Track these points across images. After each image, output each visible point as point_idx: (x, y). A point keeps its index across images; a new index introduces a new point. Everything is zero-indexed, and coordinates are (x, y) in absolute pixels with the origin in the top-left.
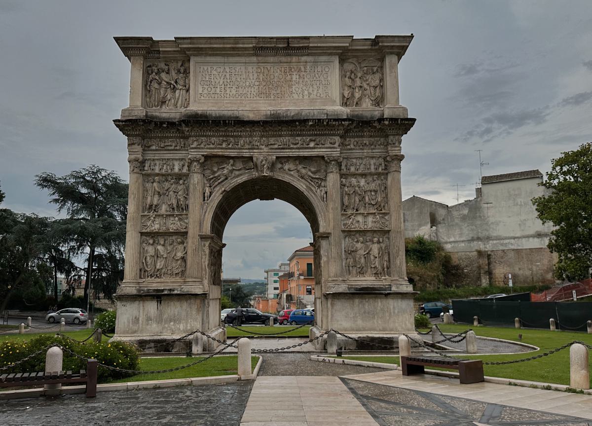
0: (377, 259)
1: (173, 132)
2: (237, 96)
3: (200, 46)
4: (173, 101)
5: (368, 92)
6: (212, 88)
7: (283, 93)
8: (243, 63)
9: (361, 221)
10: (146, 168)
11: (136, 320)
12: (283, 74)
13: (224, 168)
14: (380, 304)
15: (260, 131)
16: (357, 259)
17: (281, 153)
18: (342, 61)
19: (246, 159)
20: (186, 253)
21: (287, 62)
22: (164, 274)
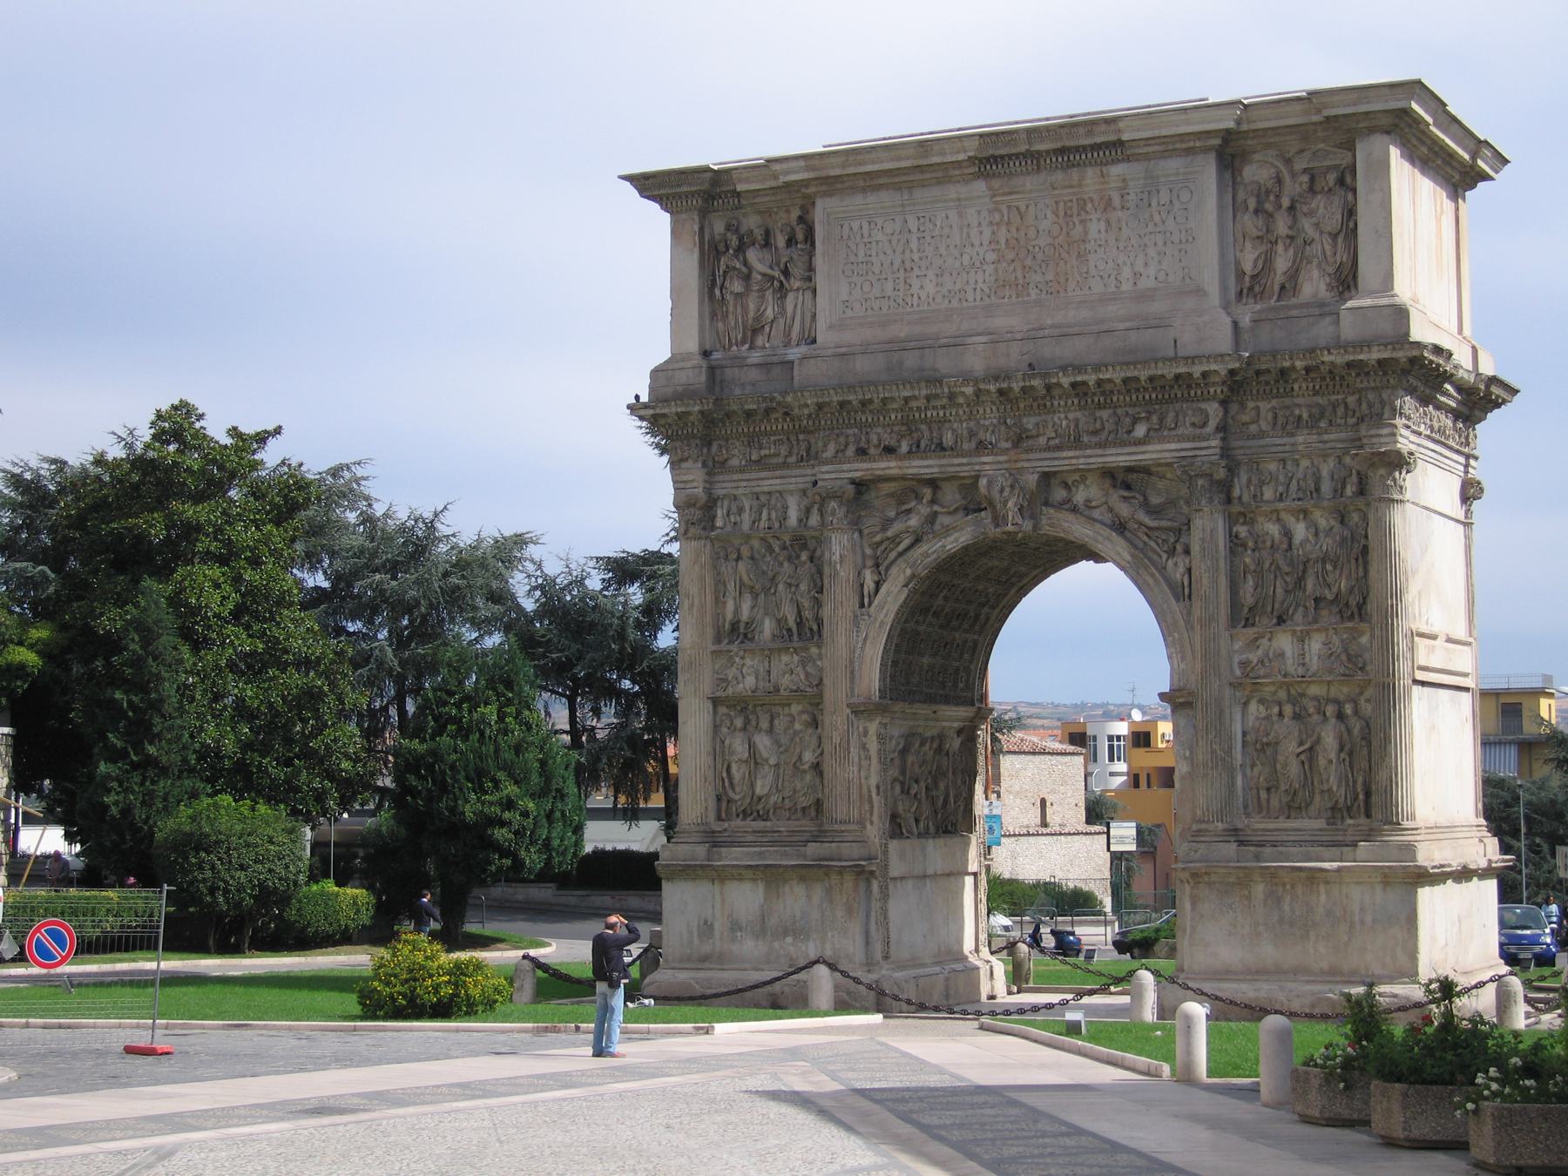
0: (1333, 767)
2: (939, 299)
3: (833, 173)
4: (782, 321)
5: (1316, 248)
7: (1062, 281)
8: (953, 200)
9: (1289, 652)
10: (719, 523)
11: (707, 928)
14: (1323, 898)
16: (1278, 766)
17: (1056, 463)
20: (822, 754)
21: (1071, 187)
22: (775, 809)
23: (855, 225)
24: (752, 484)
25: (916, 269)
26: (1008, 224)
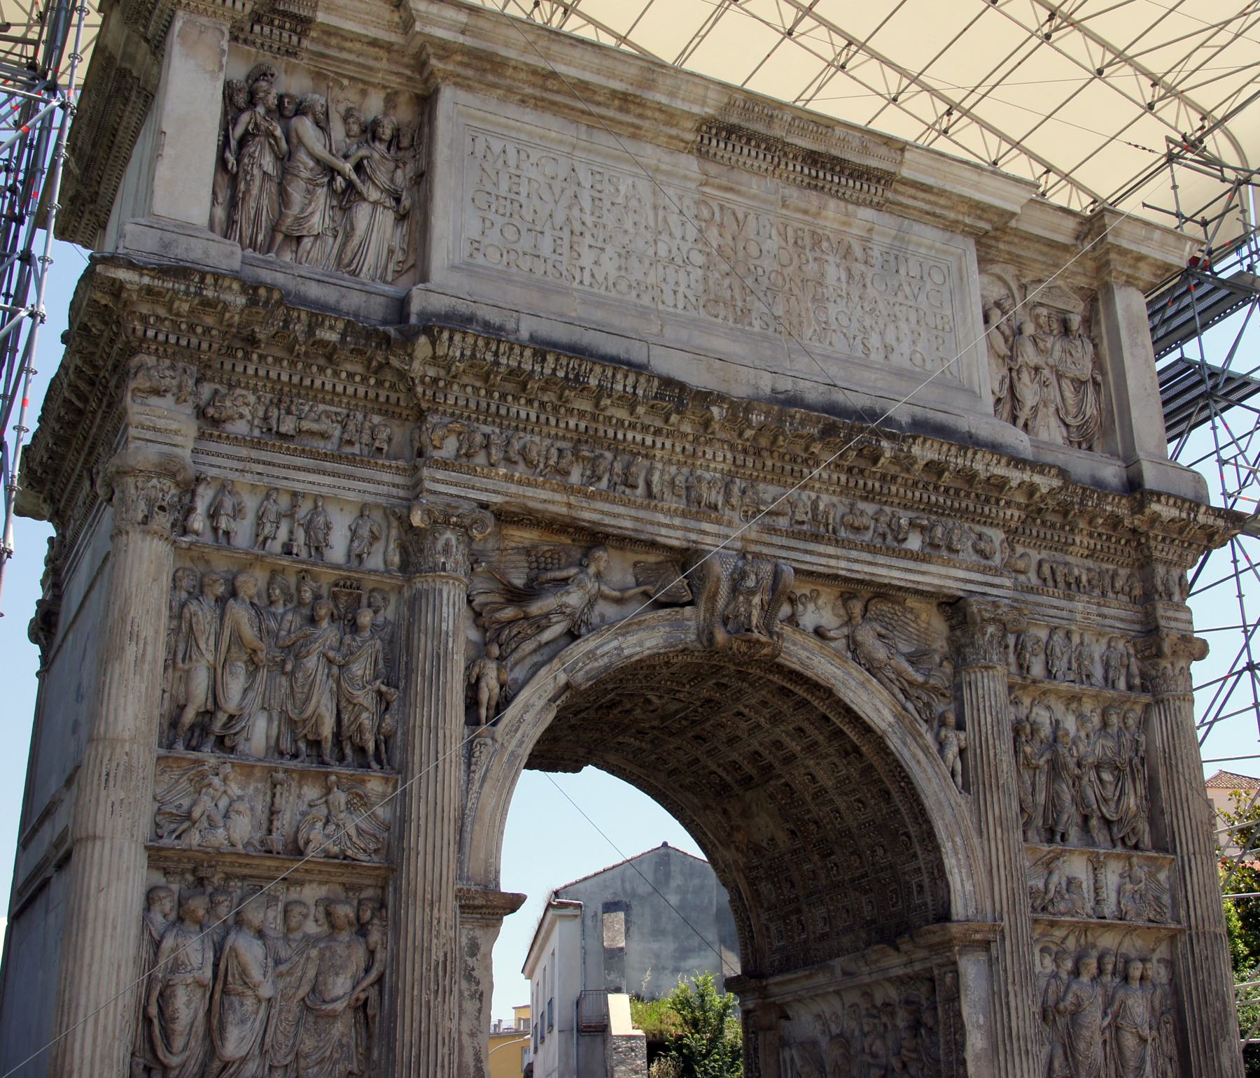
1: (351, 375)
2: (623, 286)
7: (795, 321)
12: (790, 246)
13: (565, 581)
15: (732, 447)
17: (808, 558)
19: (652, 558)
21: (806, 212)
23: (497, 146)
24: (276, 471)
25: (588, 235)
26: (721, 225)
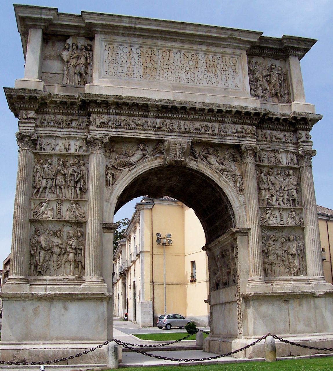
6: (119, 67)
18: (250, 55)
